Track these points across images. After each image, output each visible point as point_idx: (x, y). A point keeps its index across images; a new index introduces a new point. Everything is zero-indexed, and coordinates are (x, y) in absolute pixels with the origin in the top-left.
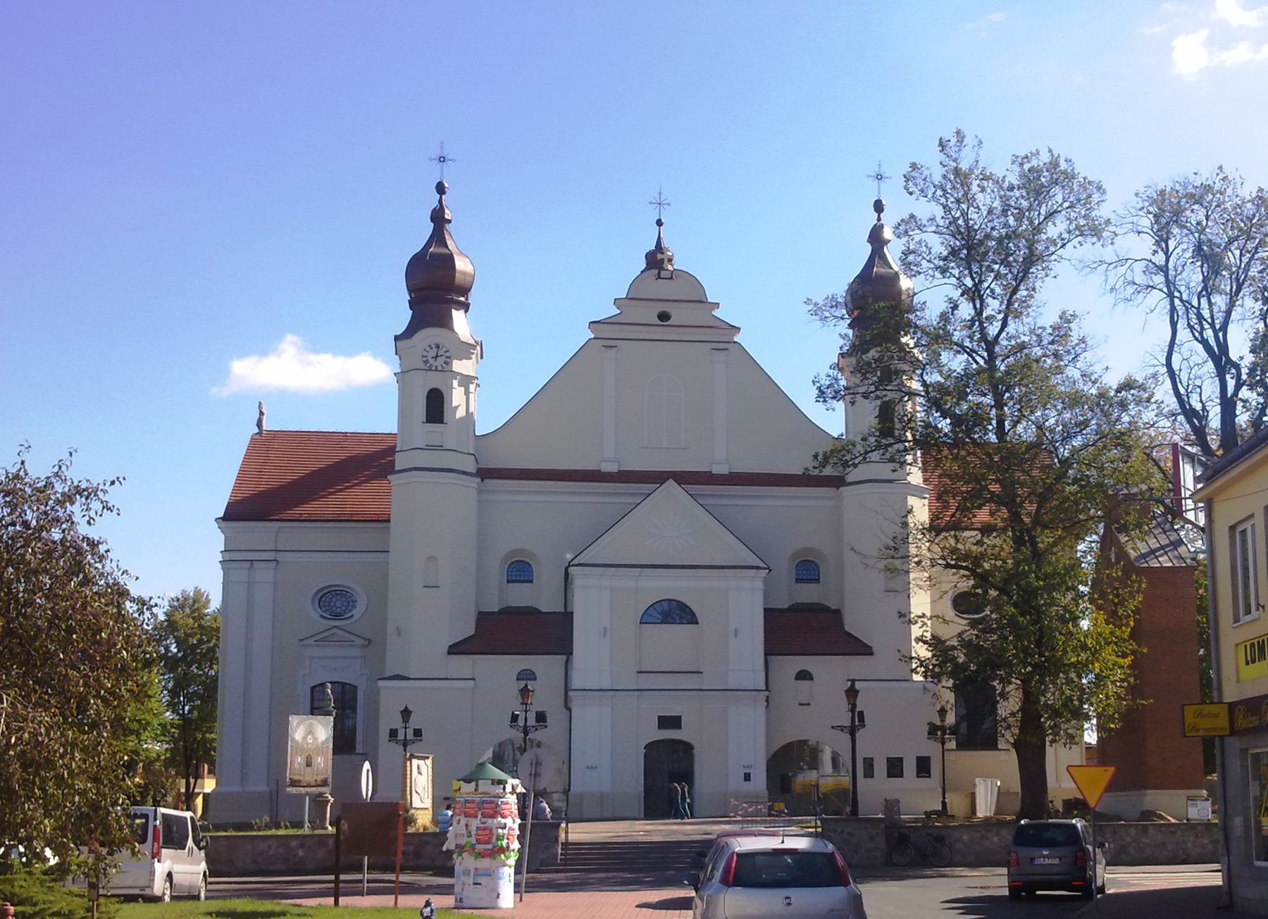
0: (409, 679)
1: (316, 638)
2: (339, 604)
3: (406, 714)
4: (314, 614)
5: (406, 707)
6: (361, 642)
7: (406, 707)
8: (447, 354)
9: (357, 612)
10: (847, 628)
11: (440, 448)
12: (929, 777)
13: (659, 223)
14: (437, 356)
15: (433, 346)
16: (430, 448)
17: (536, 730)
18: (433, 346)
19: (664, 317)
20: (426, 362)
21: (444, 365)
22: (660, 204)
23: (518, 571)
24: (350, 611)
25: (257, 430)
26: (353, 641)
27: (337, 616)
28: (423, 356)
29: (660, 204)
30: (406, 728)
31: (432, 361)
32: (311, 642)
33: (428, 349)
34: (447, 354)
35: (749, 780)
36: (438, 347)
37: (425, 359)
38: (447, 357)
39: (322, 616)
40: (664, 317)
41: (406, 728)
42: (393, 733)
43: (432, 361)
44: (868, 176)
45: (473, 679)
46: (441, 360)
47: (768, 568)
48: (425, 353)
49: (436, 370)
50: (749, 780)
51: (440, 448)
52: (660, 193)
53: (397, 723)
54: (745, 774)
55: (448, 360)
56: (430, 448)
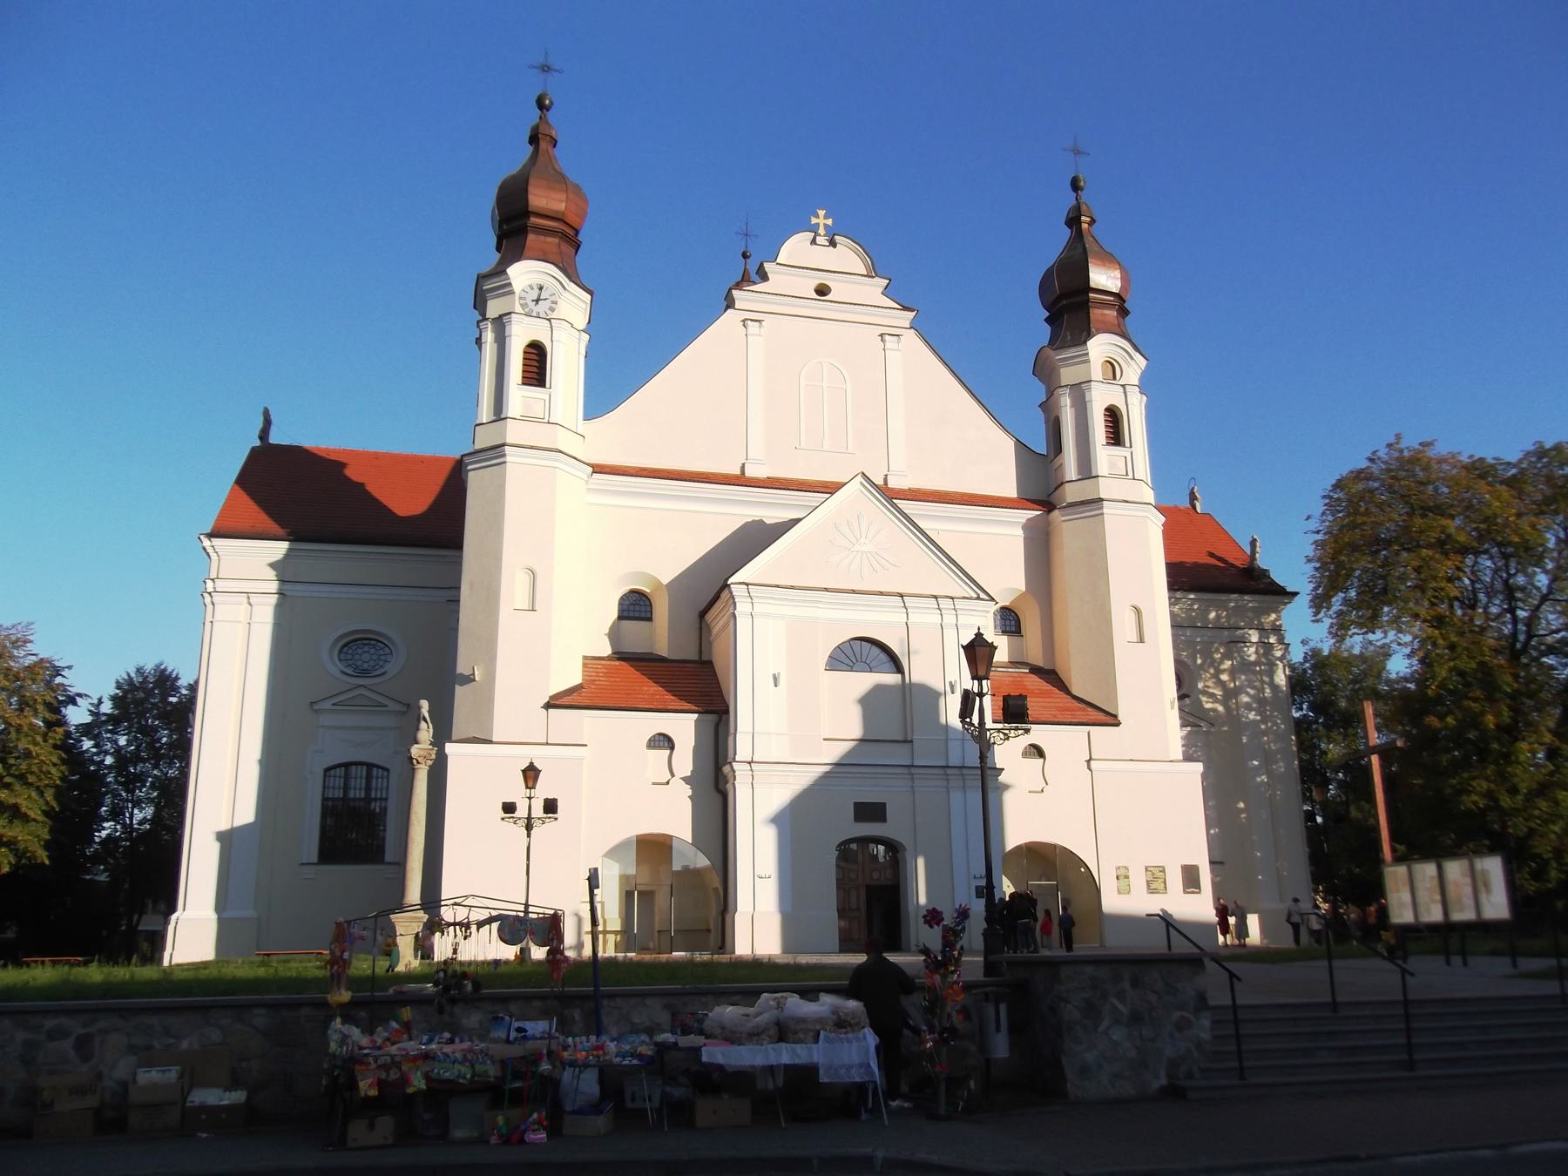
1: (335, 700)
2: (366, 657)
3: (531, 774)
4: (334, 667)
6: (398, 707)
8: (553, 298)
9: (393, 667)
10: (1075, 692)
14: (537, 301)
17: (1007, 738)
18: (535, 287)
19: (822, 291)
22: (747, 235)
24: (382, 667)
25: (257, 443)
27: (364, 673)
29: (747, 235)
30: (530, 798)
32: (327, 705)
33: (528, 289)
36: (541, 288)
37: (522, 302)
38: (554, 302)
39: (342, 672)
40: (822, 291)
41: (530, 798)
44: (1065, 150)
47: (993, 599)
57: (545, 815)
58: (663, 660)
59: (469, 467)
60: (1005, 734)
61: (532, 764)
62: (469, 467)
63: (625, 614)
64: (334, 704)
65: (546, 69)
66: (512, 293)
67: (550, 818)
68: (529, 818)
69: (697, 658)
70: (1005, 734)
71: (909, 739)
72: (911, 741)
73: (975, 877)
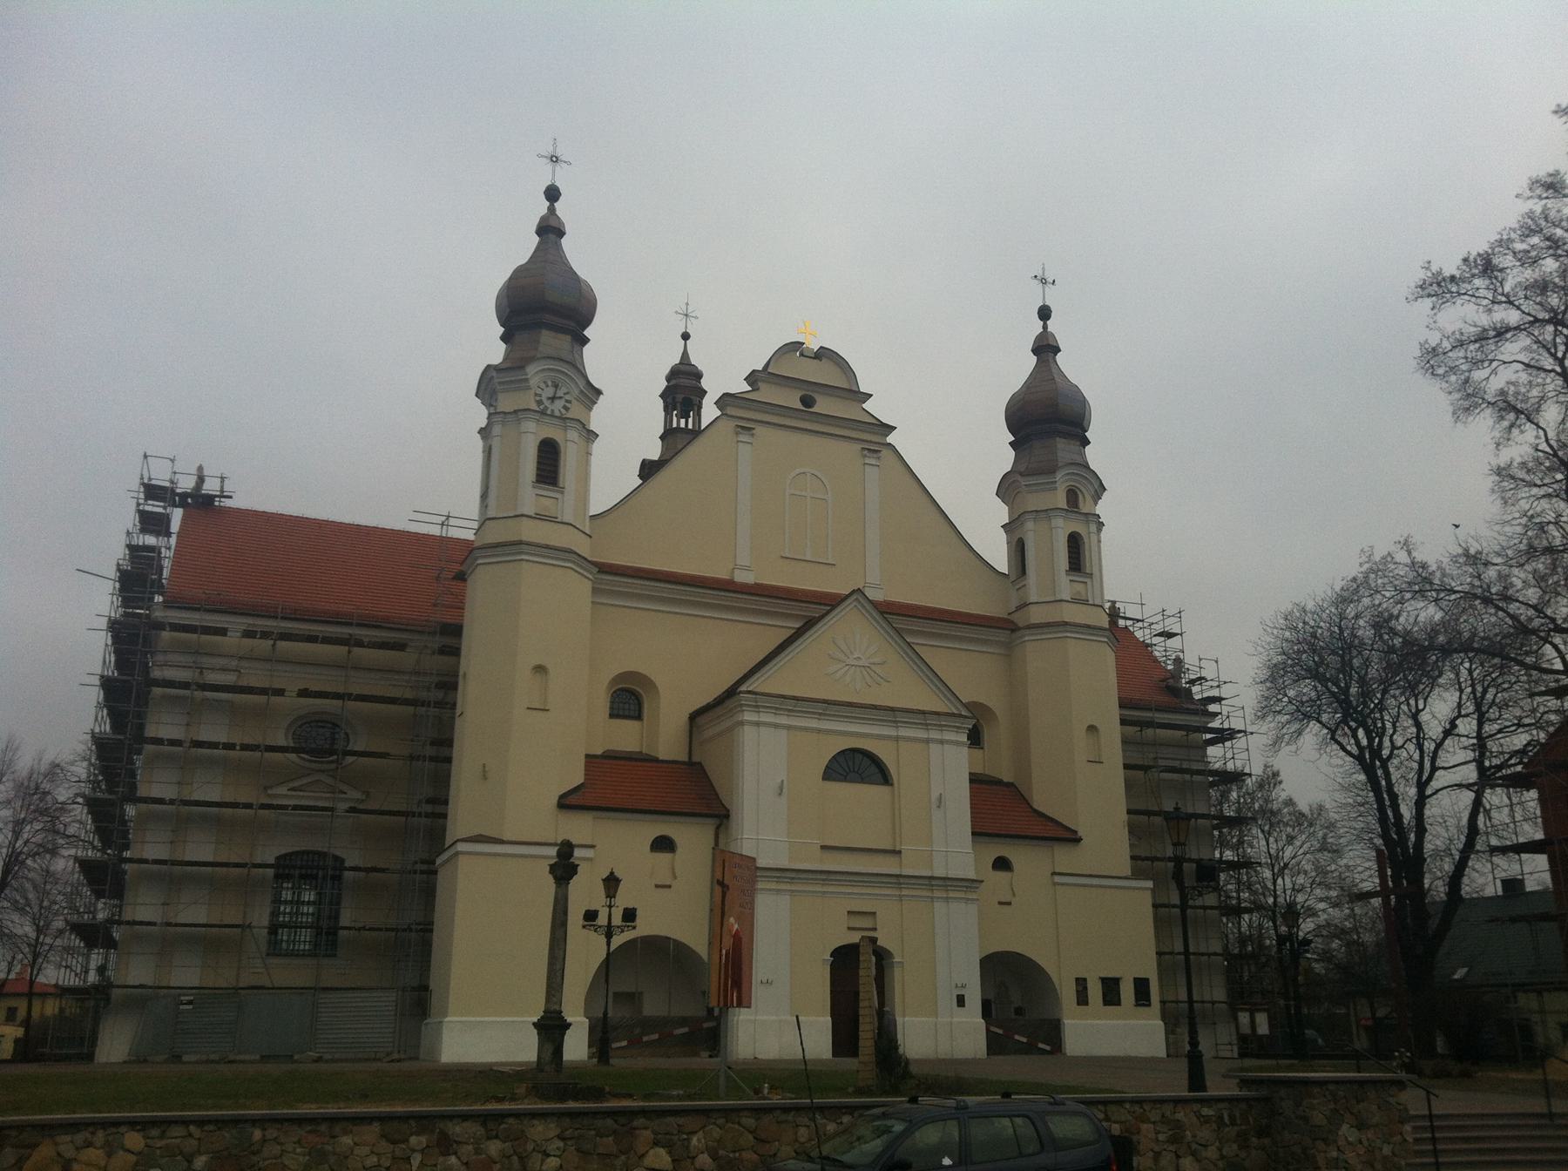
0: (502, 842)
3: (612, 883)
5: (612, 873)
7: (612, 873)
8: (567, 397)
11: (552, 519)
12: (1149, 1005)
13: (686, 336)
14: (553, 399)
15: (550, 383)
16: (539, 517)
18: (550, 383)
20: (539, 403)
21: (563, 411)
22: (686, 315)
23: (622, 702)
26: (345, 793)
28: (536, 395)
30: (610, 907)
31: (547, 403)
33: (543, 386)
34: (567, 397)
35: (1086, 1003)
37: (538, 398)
38: (567, 401)
40: (807, 401)
41: (610, 907)
42: (590, 916)
43: (547, 403)
45: (593, 847)
46: (559, 404)
48: (539, 391)
49: (552, 415)
50: (1086, 1003)
51: (552, 519)
52: (687, 304)
53: (598, 901)
54: (958, 996)
55: (567, 404)
56: (539, 517)
57: (624, 924)
58: (656, 760)
59: (480, 561)
60: (1198, 891)
61: (612, 873)
62: (480, 561)
63: (615, 712)
64: (293, 789)
65: (554, 159)
66: (529, 388)
67: (628, 926)
68: (609, 925)
69: (687, 760)
70: (1198, 891)
71: (897, 849)
72: (900, 852)
73: (957, 986)
